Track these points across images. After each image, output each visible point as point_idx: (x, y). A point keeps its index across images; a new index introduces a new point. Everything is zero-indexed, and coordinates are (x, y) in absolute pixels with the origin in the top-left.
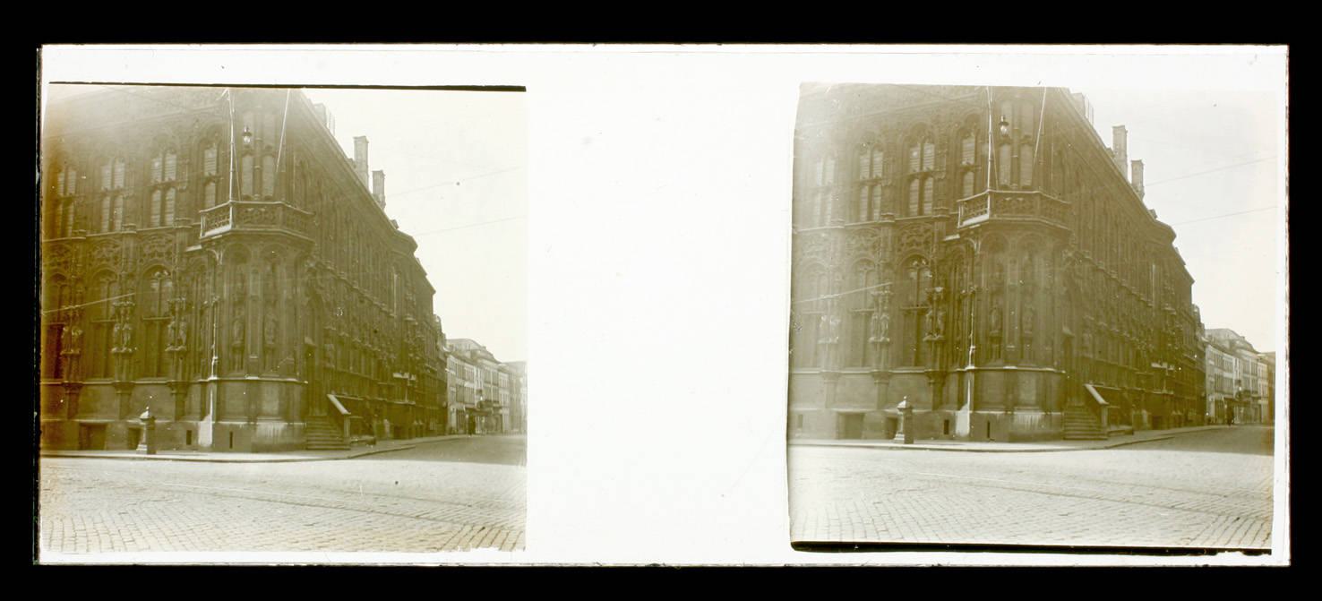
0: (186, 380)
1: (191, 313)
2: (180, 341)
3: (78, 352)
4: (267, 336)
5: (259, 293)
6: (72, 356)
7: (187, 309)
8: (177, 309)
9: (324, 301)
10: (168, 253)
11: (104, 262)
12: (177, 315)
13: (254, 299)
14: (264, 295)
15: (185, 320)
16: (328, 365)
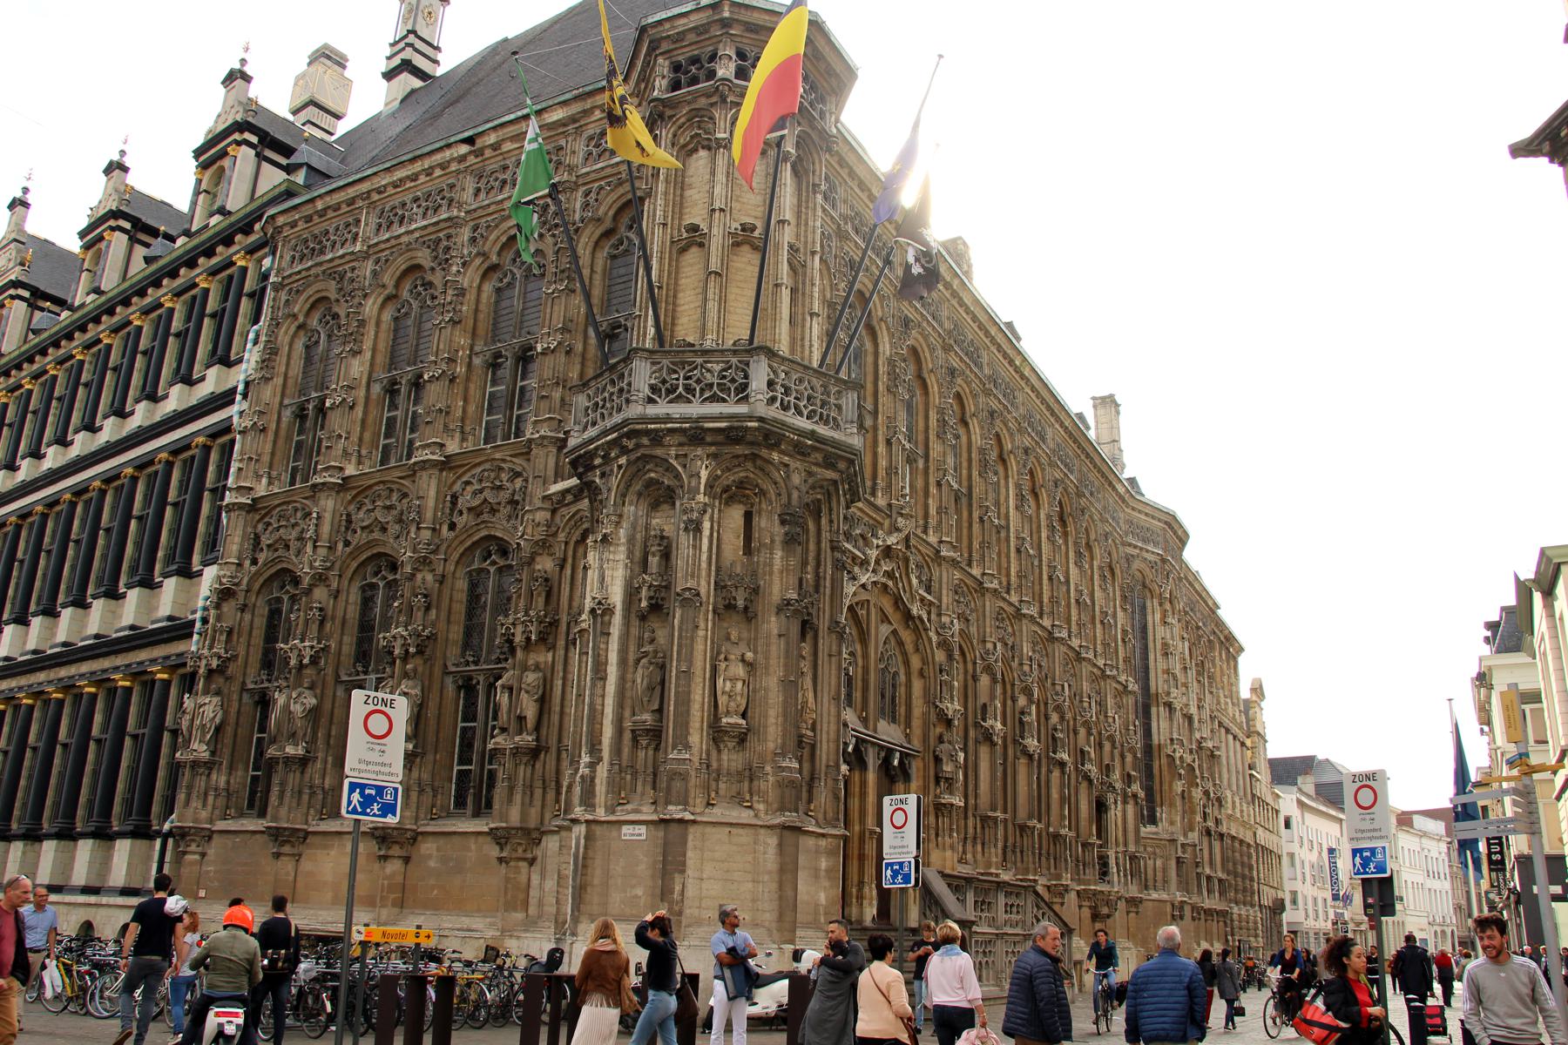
0: (532, 824)
1: (553, 647)
2: (521, 719)
3: (300, 751)
4: (722, 700)
5: (705, 587)
6: (288, 760)
7: (542, 639)
8: (518, 639)
9: (934, 638)
10: (513, 502)
11: (376, 535)
12: (519, 654)
13: (691, 600)
14: (719, 586)
15: (537, 668)
16: (947, 799)
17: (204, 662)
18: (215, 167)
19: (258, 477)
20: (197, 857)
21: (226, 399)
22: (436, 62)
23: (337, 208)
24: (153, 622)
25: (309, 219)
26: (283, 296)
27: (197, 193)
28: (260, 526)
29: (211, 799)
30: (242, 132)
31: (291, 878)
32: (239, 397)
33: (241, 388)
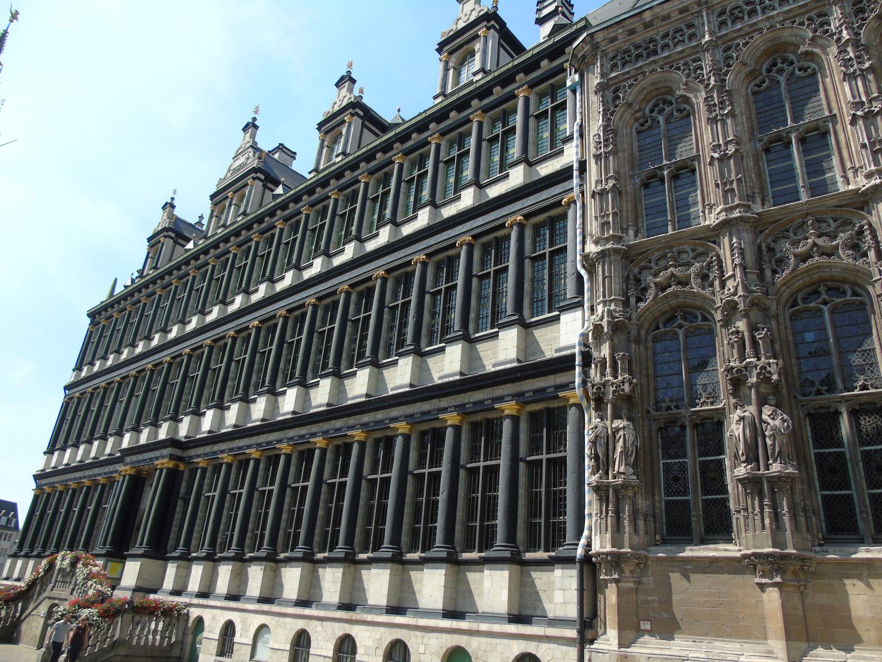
17: (612, 389)
18: (461, 50)
19: (625, 230)
20: (631, 585)
21: (564, 174)
22: (573, 14)
23: (667, 17)
24: (494, 366)
25: (632, 32)
26: (610, 95)
27: (446, 70)
28: (636, 270)
29: (641, 523)
30: (488, 22)
31: (800, 613)
32: (575, 173)
33: (576, 166)
